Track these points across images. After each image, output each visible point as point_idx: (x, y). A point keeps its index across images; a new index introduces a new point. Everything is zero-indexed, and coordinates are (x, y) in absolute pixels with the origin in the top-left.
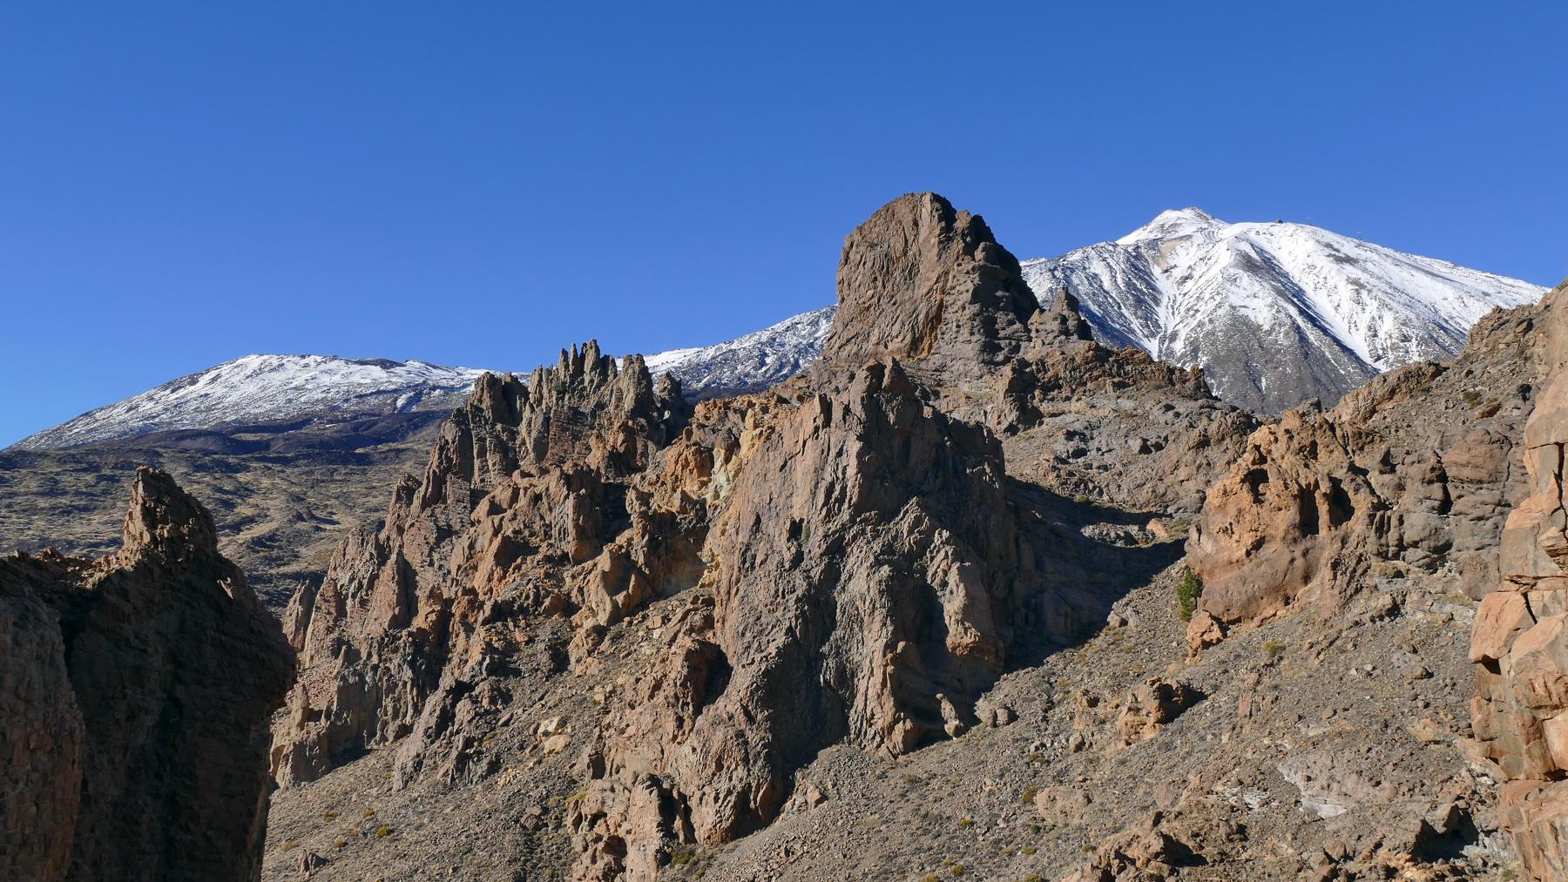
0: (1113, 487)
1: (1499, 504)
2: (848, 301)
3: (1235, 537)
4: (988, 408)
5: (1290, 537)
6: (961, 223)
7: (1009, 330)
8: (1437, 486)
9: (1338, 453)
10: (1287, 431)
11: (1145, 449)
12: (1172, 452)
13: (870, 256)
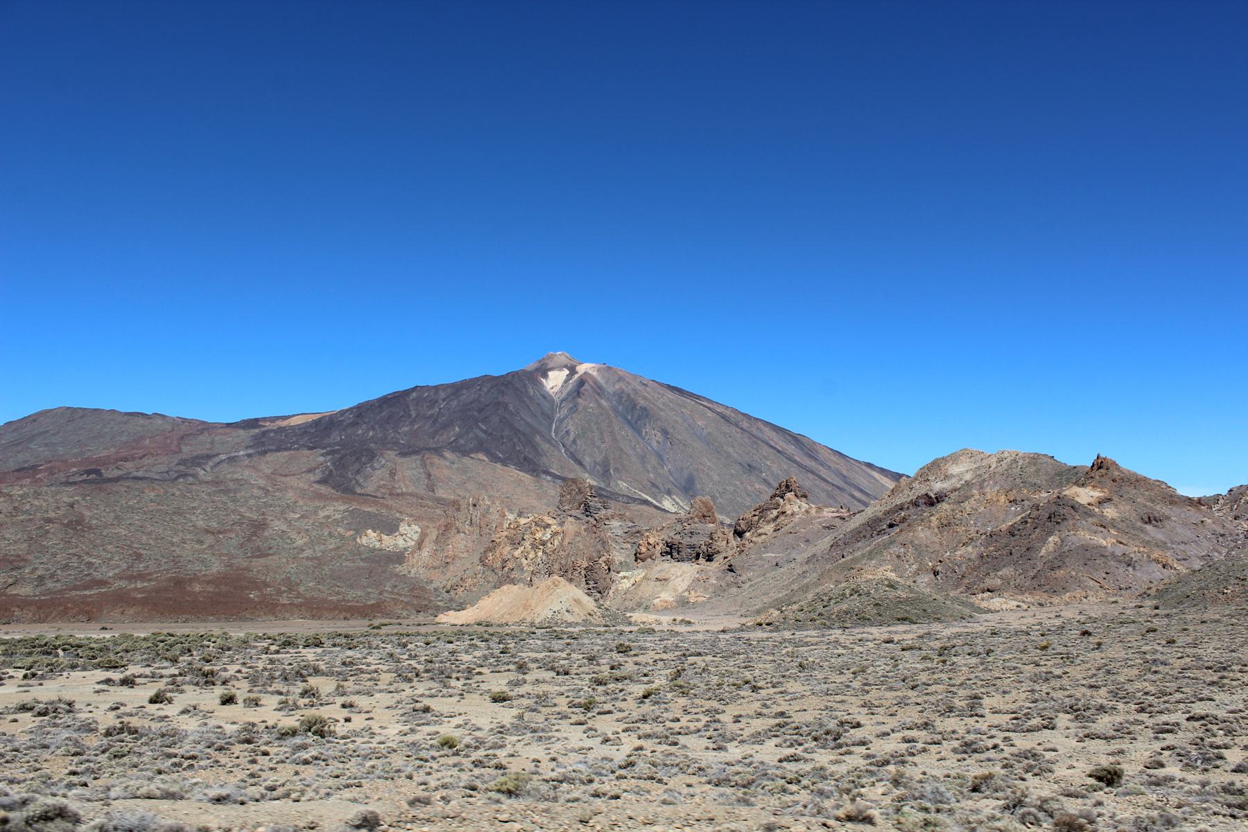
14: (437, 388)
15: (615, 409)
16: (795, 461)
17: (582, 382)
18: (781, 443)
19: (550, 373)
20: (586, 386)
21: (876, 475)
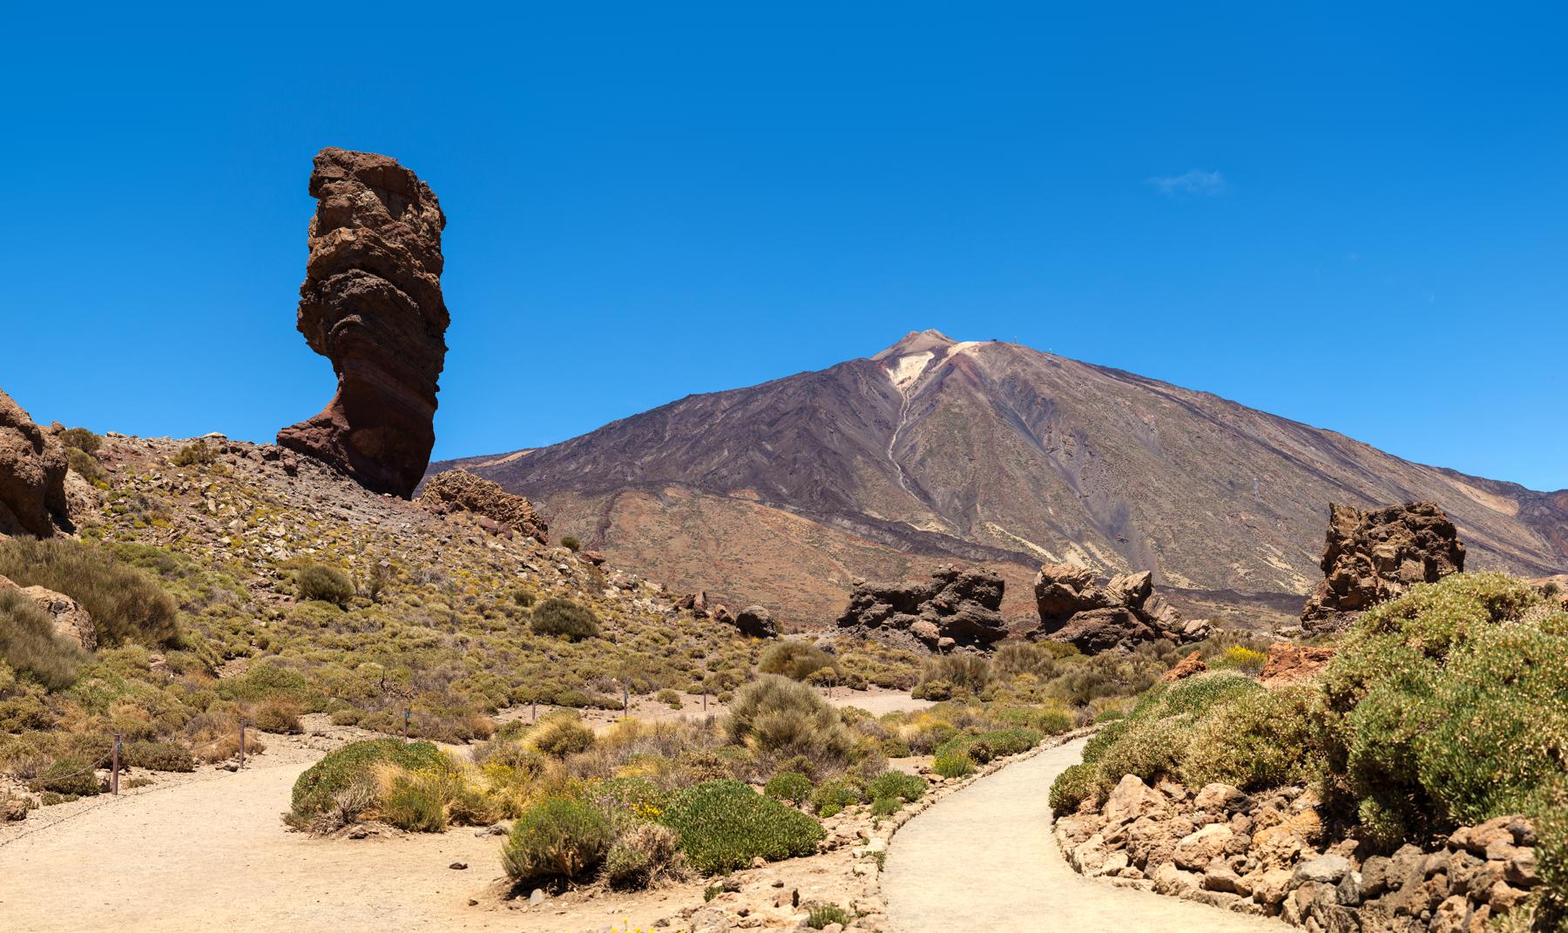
14: (717, 396)
15: (1000, 409)
16: (1314, 471)
17: (950, 367)
18: (1292, 444)
19: (904, 362)
20: (956, 374)
21: (1462, 487)
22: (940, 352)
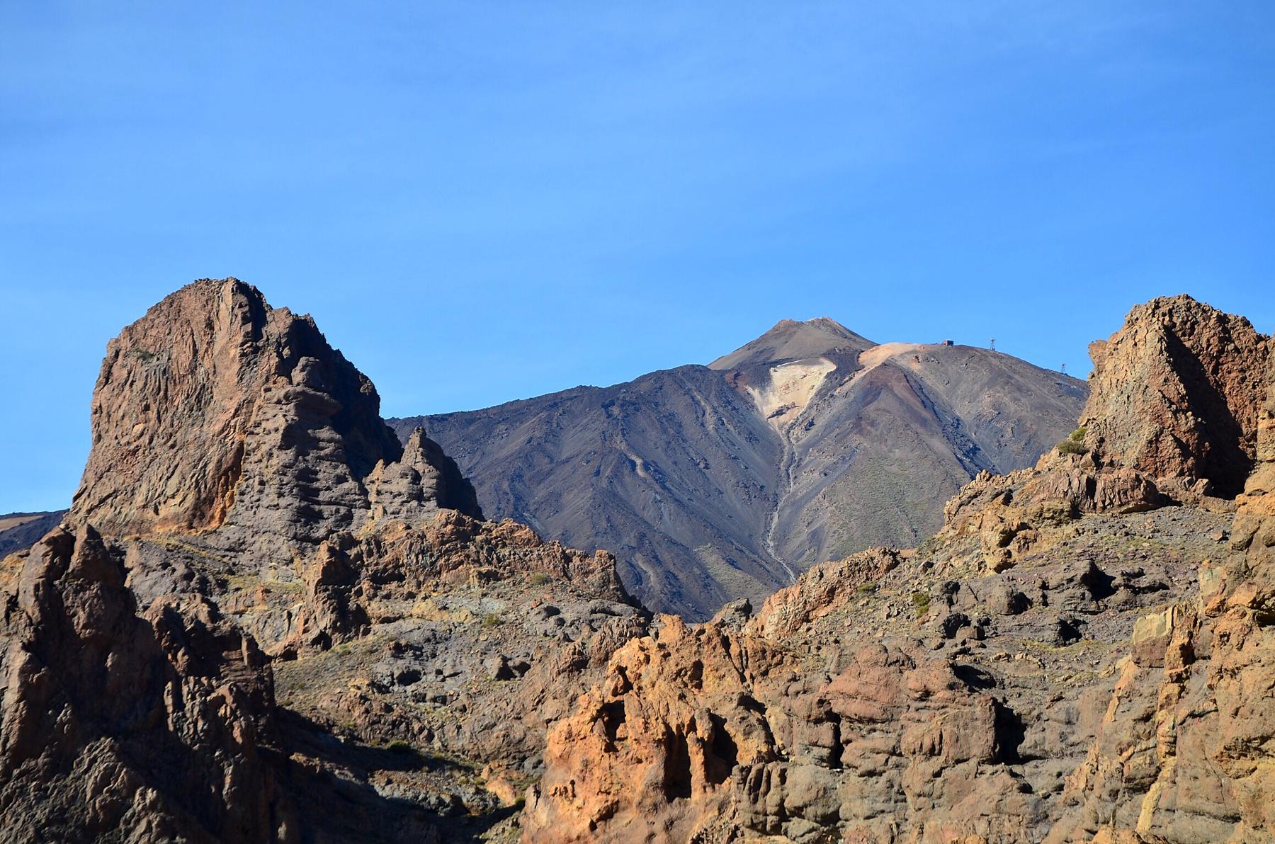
0: (450, 730)
1: (893, 752)
2: (106, 440)
3: (578, 802)
4: (295, 608)
5: (648, 801)
6: (276, 328)
7: (338, 491)
8: (827, 727)
9: (732, 684)
10: (661, 647)
11: (505, 673)
12: (537, 678)
13: (141, 371)
17: (872, 390)
19: (780, 375)
20: (884, 401)
22: (846, 362)
